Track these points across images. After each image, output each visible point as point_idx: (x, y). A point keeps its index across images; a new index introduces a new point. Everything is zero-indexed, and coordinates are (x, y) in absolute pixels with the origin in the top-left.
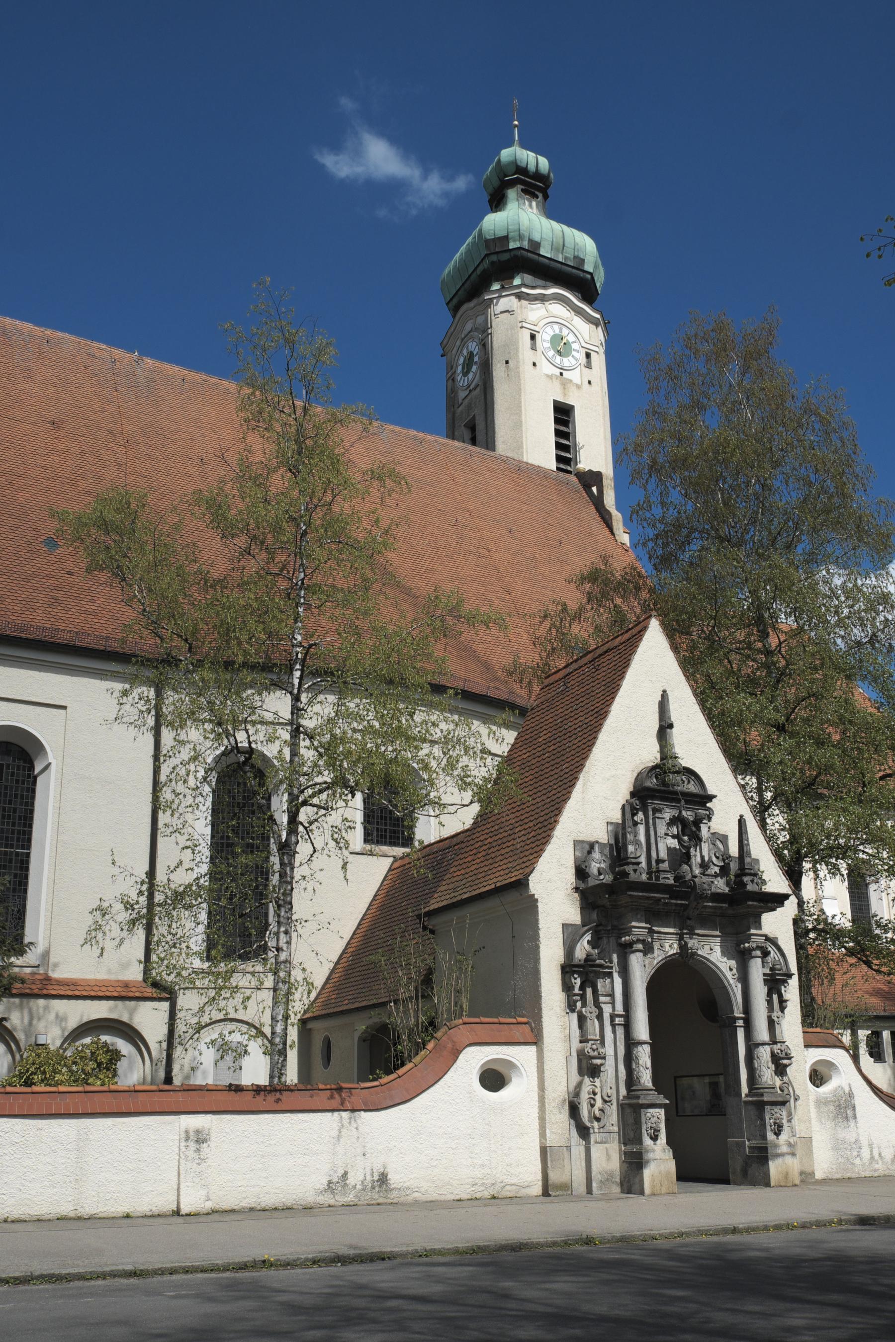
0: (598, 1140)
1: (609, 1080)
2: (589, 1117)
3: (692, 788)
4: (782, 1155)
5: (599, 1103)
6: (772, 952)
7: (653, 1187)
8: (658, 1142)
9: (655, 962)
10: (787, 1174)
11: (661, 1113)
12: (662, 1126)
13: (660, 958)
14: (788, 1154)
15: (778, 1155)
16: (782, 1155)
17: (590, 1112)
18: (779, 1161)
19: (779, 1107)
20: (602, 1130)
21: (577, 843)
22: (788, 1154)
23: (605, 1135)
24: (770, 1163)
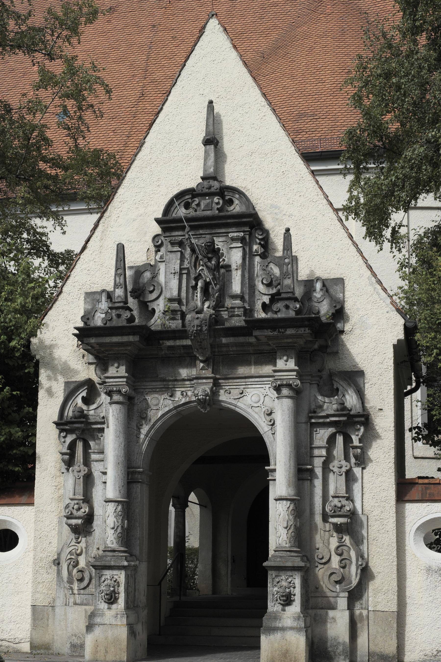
0: (78, 601)
1: (96, 541)
2: (68, 578)
3: (237, 208)
4: (283, 629)
5: (82, 563)
6: (341, 388)
7: (96, 651)
8: (114, 606)
9: (160, 414)
10: (287, 651)
11: (121, 576)
12: (122, 589)
13: (167, 409)
14: (292, 628)
15: (275, 629)
16: (283, 629)
17: (70, 573)
18: (278, 635)
19: (289, 573)
20: (82, 592)
21: (88, 295)
22: (292, 628)
23: (87, 597)
24: (263, 638)
